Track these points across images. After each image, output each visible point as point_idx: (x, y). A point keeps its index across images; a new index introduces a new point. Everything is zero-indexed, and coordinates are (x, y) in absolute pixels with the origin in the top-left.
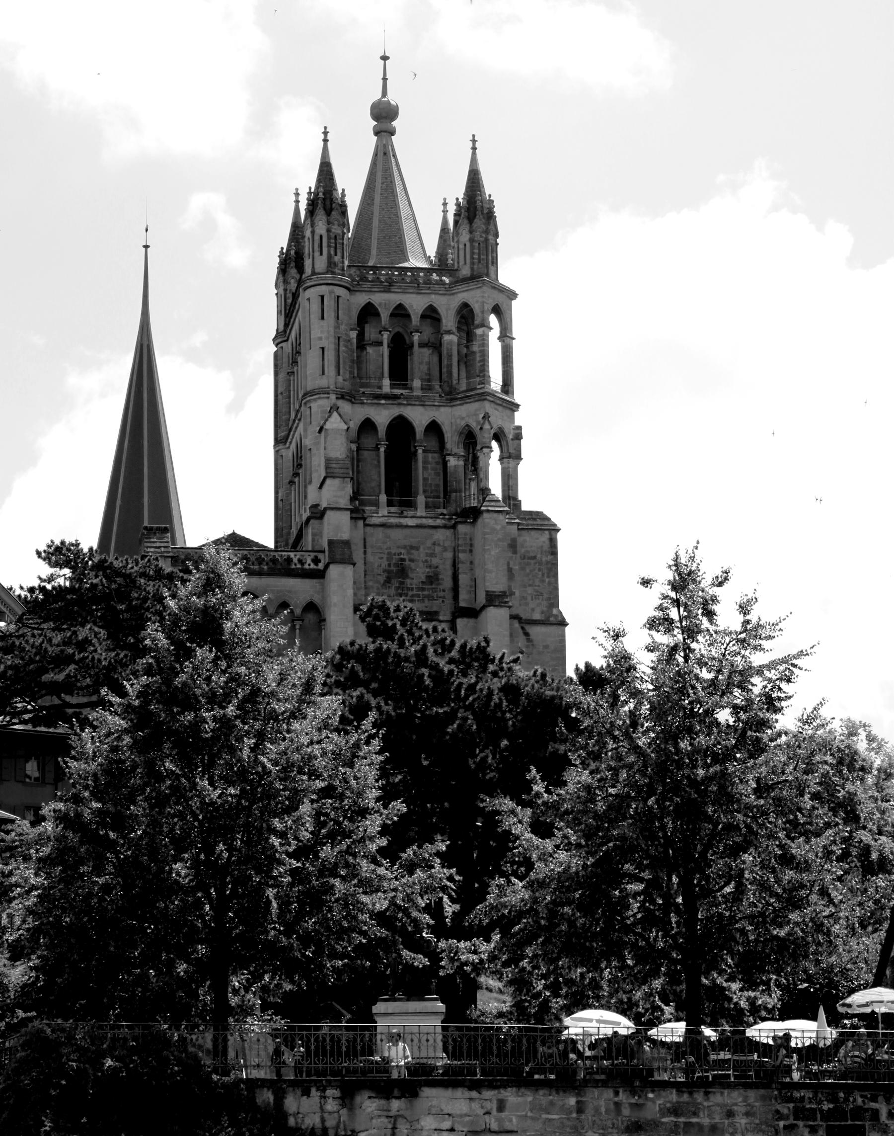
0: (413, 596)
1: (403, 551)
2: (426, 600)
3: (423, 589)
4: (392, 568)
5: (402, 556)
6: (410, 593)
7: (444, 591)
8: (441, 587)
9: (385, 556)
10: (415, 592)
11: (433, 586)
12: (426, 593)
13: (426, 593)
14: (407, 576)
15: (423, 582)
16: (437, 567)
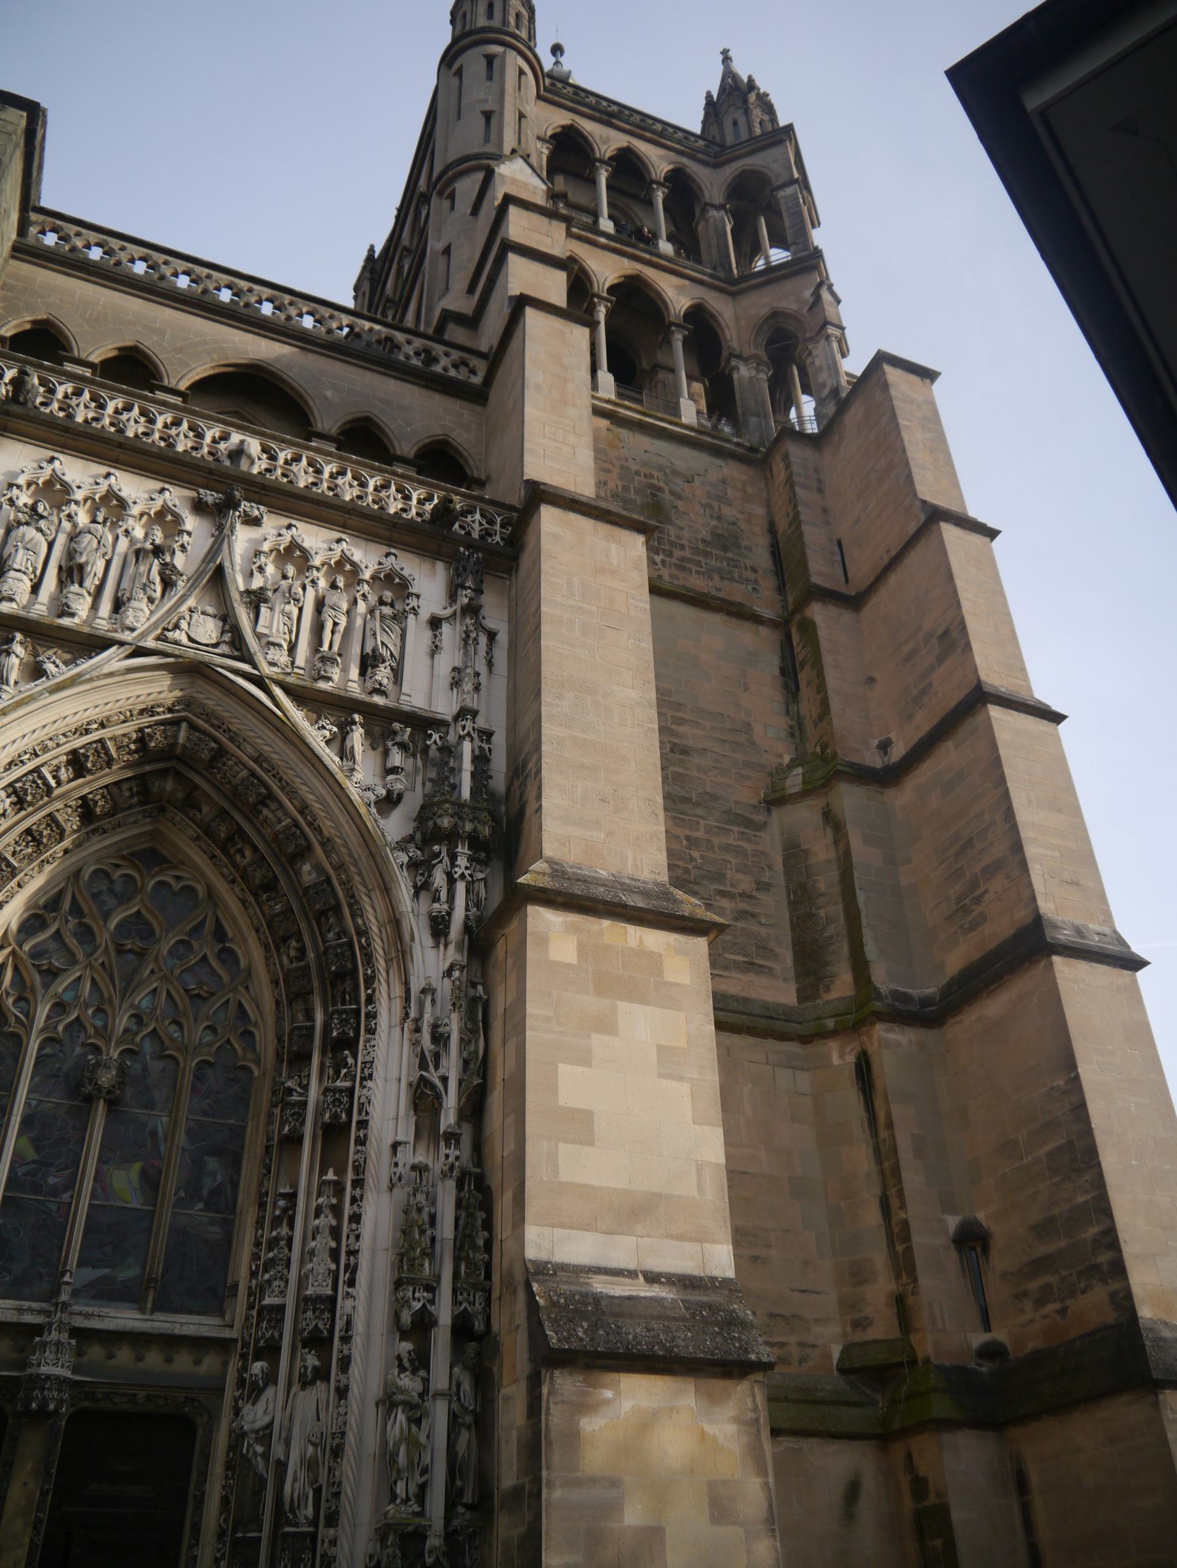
0: (682, 559)
1: (656, 474)
2: (716, 577)
3: (707, 554)
4: (632, 495)
5: (654, 482)
6: (677, 553)
7: (754, 570)
8: (748, 562)
9: (616, 471)
10: (688, 554)
11: (730, 555)
12: (713, 562)
13: (713, 562)
14: (669, 521)
15: (704, 541)
16: (734, 524)
